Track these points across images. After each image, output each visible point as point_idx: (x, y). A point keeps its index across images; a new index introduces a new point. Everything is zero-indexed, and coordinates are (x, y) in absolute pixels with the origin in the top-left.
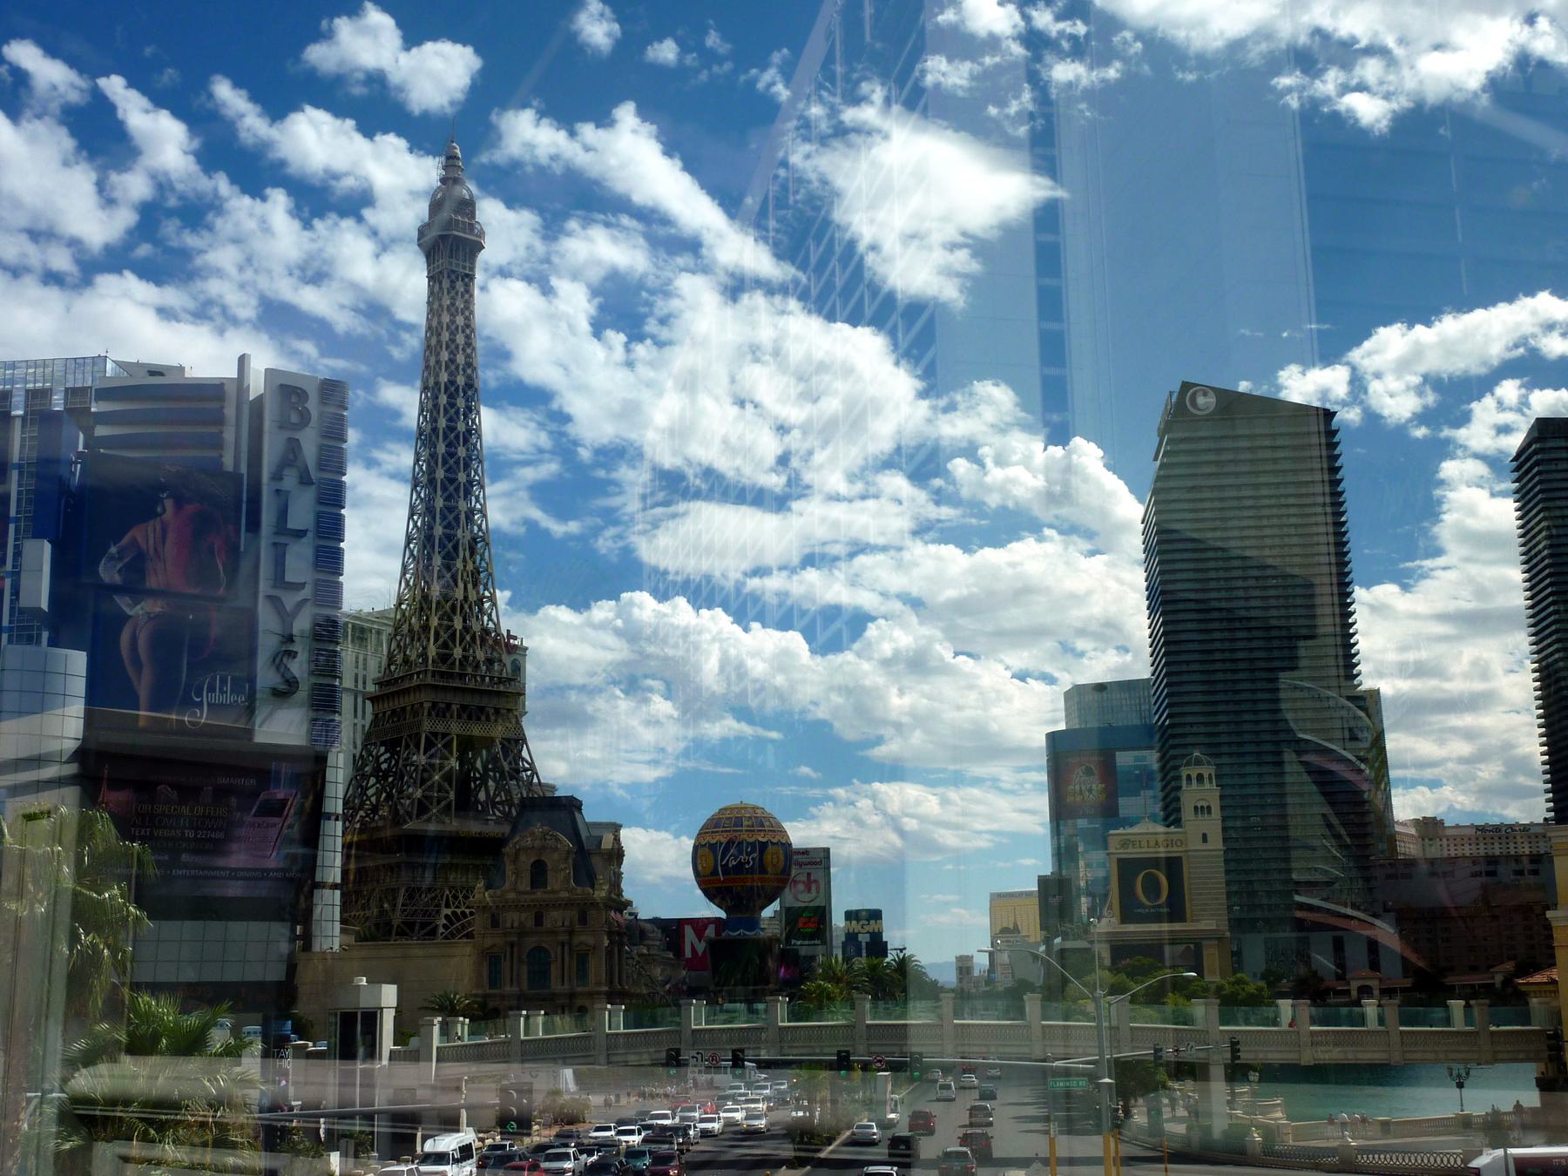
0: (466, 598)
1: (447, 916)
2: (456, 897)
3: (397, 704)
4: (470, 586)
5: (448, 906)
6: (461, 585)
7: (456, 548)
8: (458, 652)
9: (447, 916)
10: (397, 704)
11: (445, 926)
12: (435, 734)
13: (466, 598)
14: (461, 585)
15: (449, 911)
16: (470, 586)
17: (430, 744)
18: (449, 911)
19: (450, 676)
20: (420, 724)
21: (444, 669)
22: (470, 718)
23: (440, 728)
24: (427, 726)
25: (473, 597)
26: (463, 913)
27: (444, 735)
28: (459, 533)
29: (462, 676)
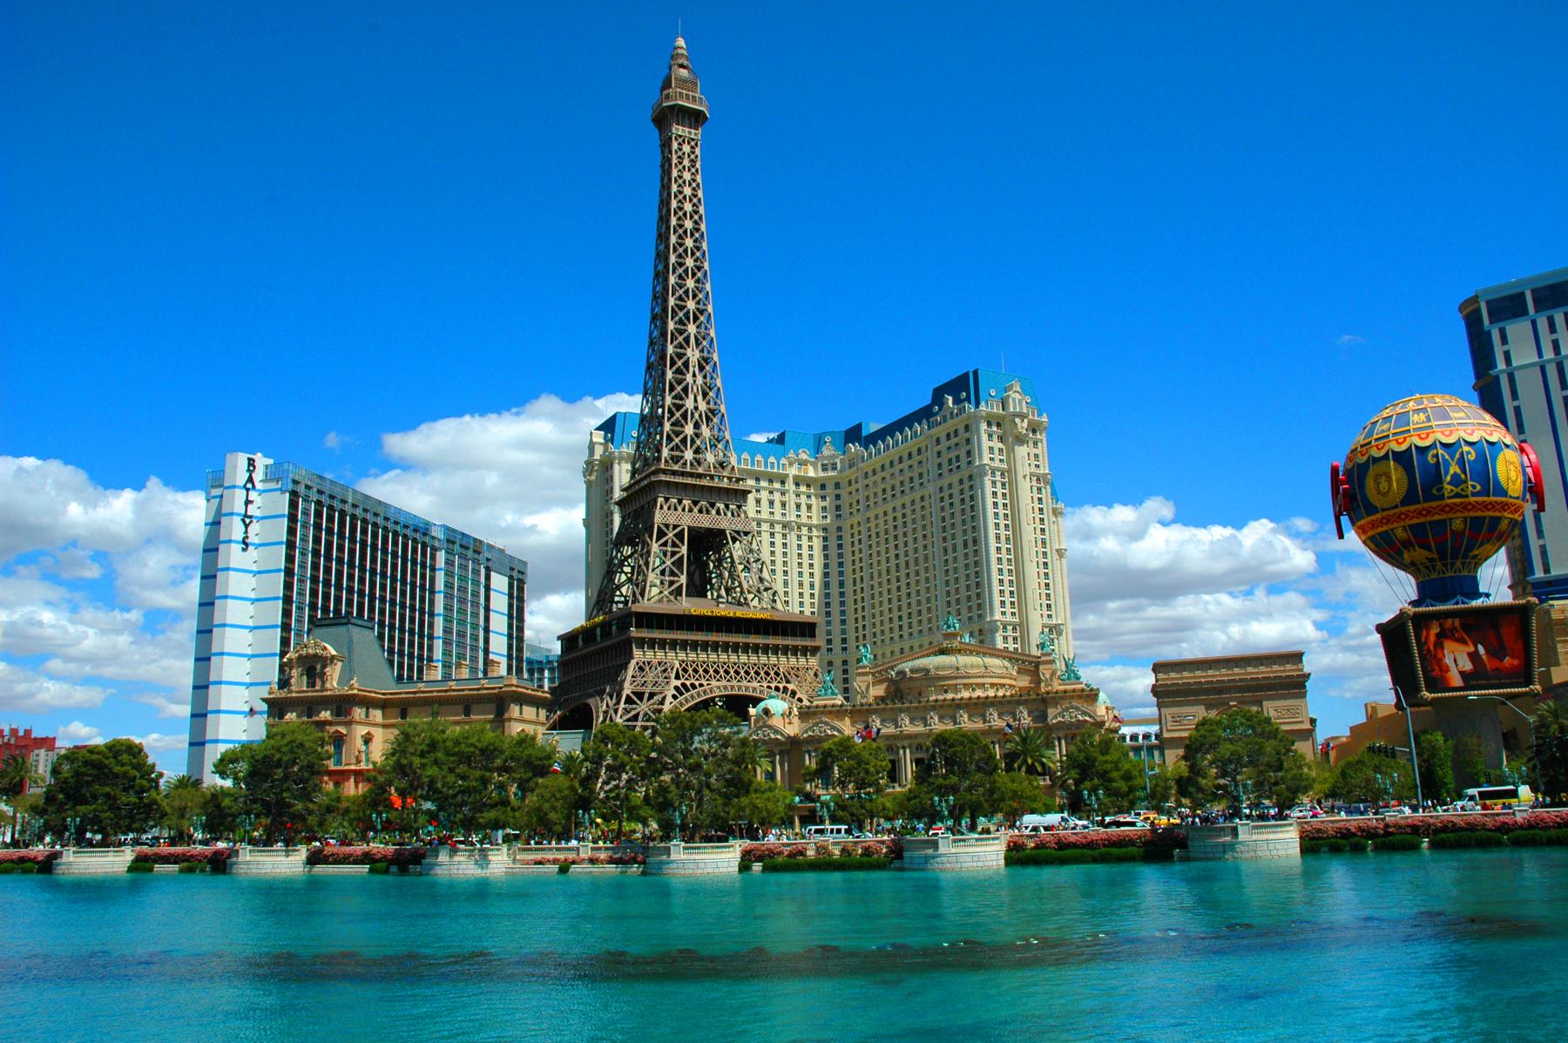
0: (696, 408)
1: (676, 688)
2: (685, 670)
3: (636, 505)
4: (700, 398)
5: (677, 677)
6: (691, 396)
7: (686, 364)
8: (689, 455)
9: (676, 688)
10: (636, 505)
11: (674, 697)
12: (667, 526)
13: (696, 408)
14: (691, 396)
15: (678, 683)
16: (700, 398)
17: (661, 534)
18: (678, 683)
19: (683, 474)
20: (652, 515)
21: (676, 468)
22: (700, 511)
23: (672, 521)
24: (658, 518)
25: (703, 406)
26: (693, 686)
27: (675, 527)
28: (689, 352)
29: (691, 475)
